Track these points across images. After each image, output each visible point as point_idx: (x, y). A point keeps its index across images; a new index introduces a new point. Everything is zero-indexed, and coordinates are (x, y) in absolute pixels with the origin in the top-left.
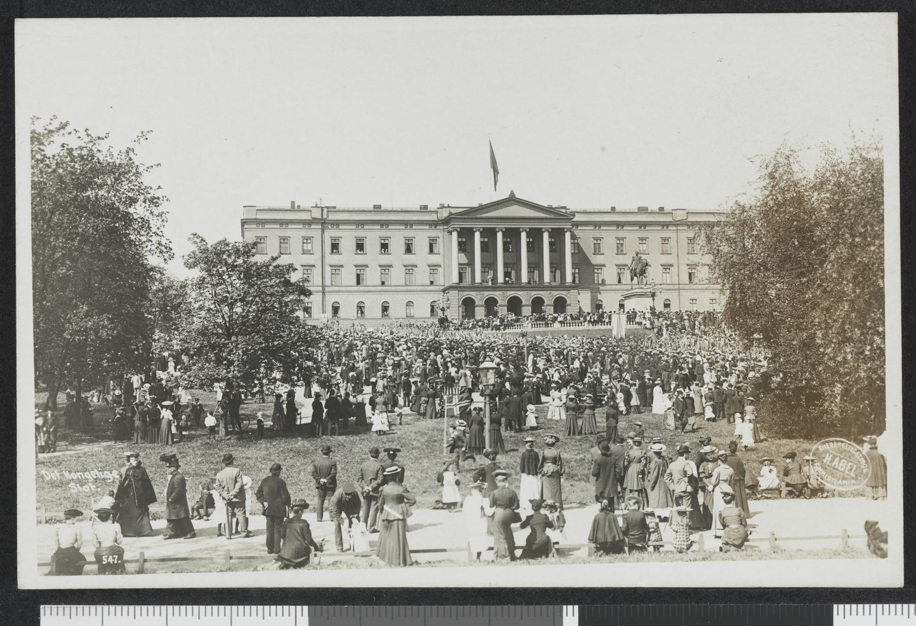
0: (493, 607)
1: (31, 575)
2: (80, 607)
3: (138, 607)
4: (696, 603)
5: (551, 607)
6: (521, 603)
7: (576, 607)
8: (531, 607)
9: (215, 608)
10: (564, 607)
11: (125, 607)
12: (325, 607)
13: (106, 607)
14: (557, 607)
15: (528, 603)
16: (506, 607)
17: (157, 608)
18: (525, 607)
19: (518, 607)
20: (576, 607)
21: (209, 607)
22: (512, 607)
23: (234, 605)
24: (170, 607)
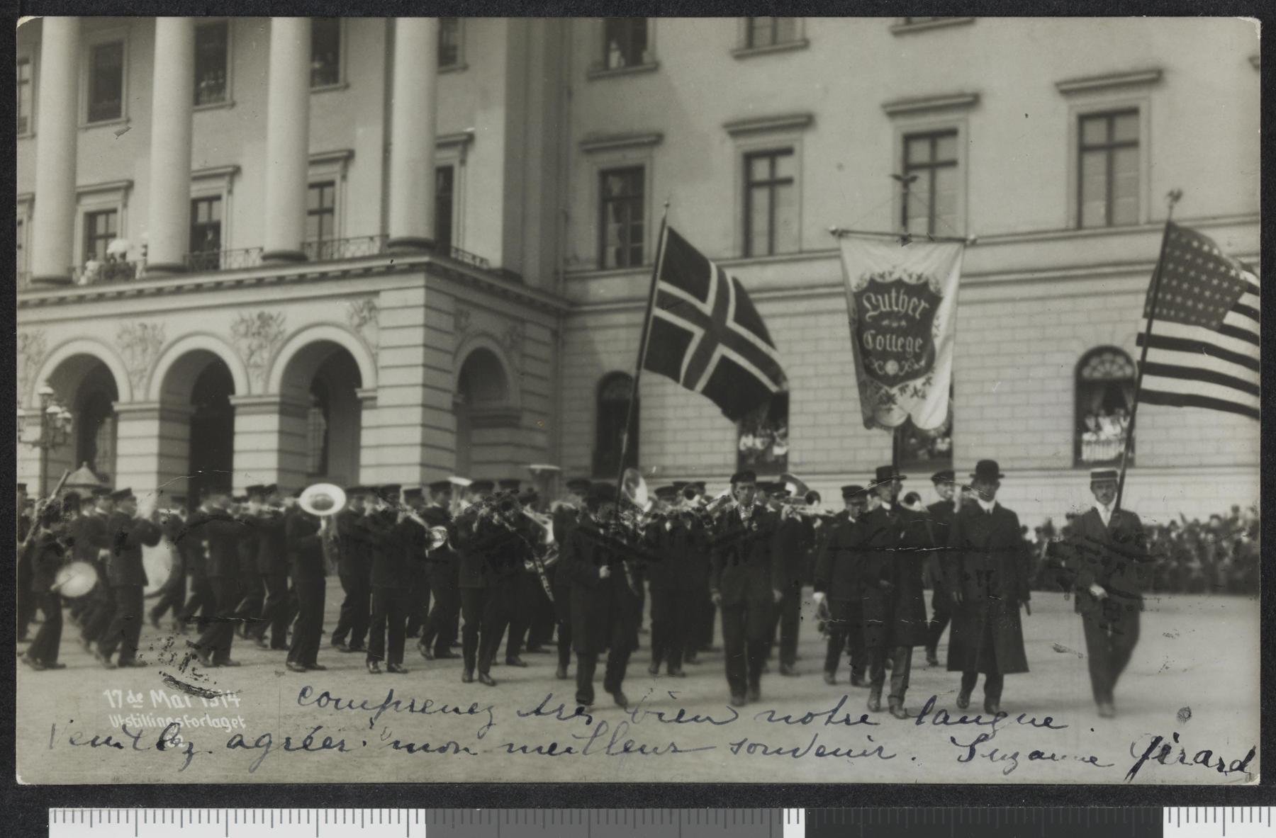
0: (684, 811)
1: (30, 769)
4: (971, 805)
6: (725, 806)
7: (802, 811)
8: (739, 811)
9: (295, 811)
10: (786, 810)
12: (449, 811)
13: (141, 811)
14: (775, 811)
16: (703, 811)
17: (213, 811)
18: (730, 811)
19: (721, 811)
20: (802, 811)
21: (286, 811)
22: (712, 811)
24: (231, 811)
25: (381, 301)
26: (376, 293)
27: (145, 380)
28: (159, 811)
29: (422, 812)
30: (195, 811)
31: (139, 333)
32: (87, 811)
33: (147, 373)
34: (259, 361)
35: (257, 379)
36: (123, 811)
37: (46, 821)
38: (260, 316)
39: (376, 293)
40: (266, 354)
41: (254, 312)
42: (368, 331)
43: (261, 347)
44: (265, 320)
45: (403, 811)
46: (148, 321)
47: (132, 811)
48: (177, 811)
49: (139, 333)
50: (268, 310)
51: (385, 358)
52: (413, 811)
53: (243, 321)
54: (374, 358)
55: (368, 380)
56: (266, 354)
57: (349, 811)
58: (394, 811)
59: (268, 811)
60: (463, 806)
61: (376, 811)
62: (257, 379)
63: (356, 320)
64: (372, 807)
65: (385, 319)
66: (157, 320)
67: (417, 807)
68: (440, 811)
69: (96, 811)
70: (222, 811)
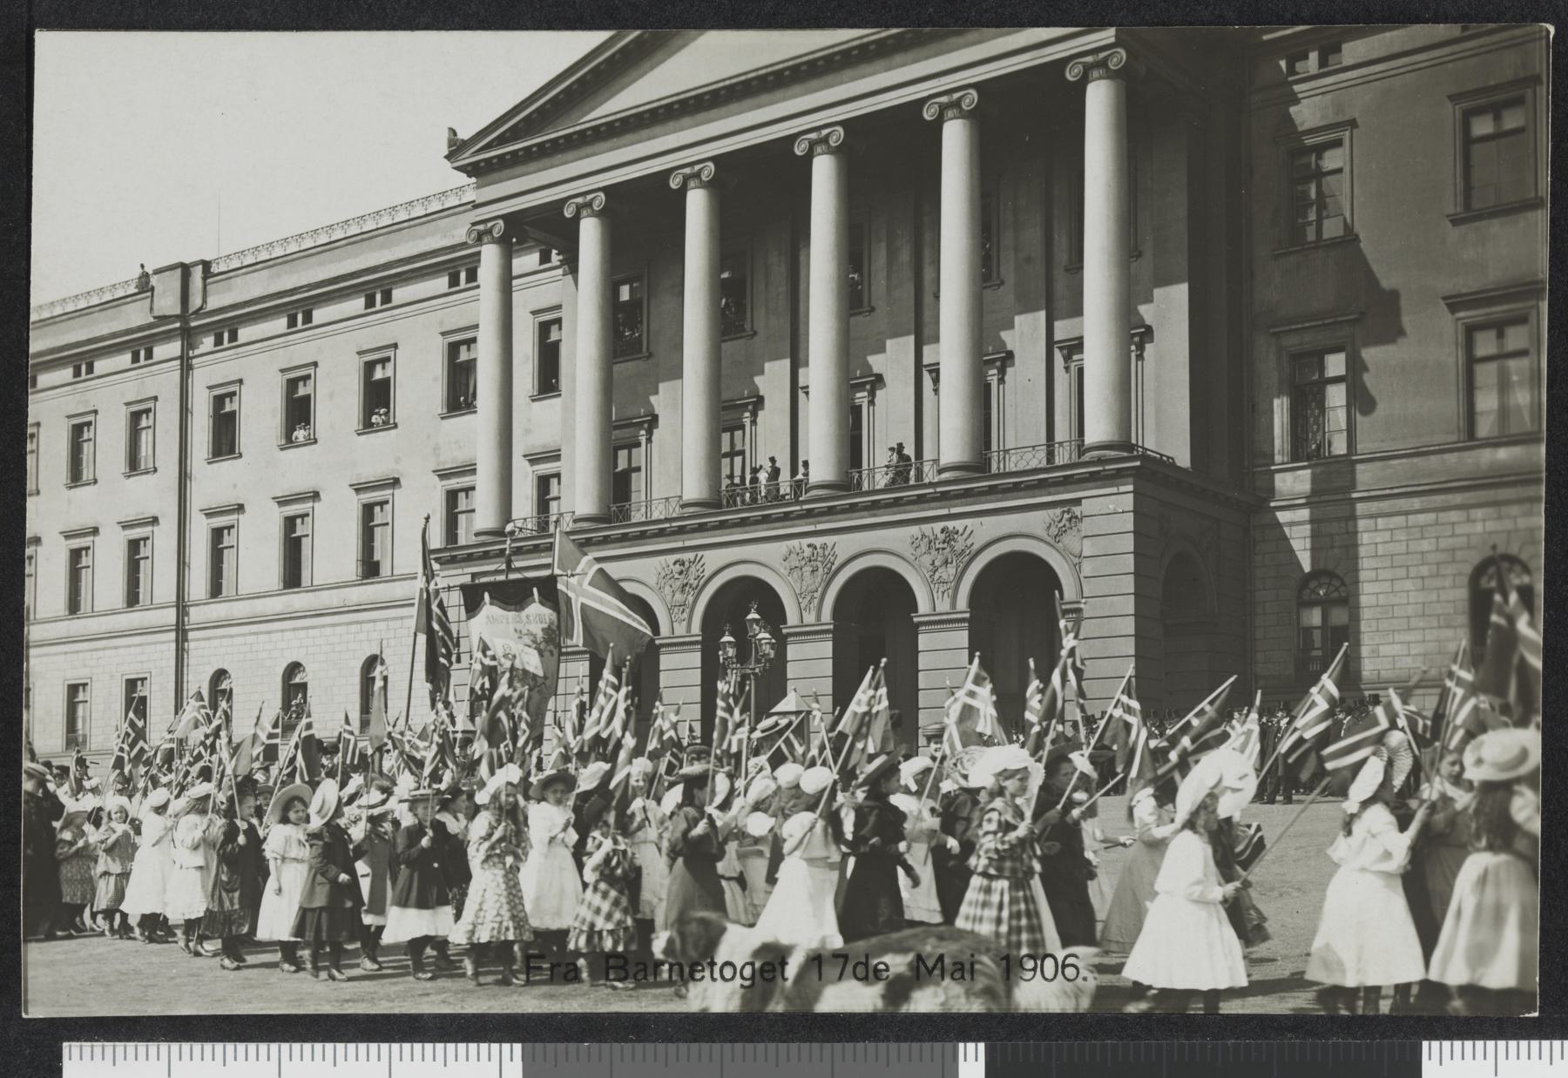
25: (1087, 507)
26: (1078, 502)
31: (808, 552)
33: (817, 595)
34: (945, 576)
35: (940, 595)
39: (1078, 502)
40: (951, 570)
41: (938, 526)
42: (1070, 540)
43: (946, 562)
44: (950, 536)
46: (818, 541)
49: (808, 552)
50: (950, 524)
51: (1087, 568)
53: (923, 536)
54: (1077, 567)
55: (1069, 592)
56: (951, 570)
63: (1054, 531)
65: (1086, 527)
66: (829, 540)
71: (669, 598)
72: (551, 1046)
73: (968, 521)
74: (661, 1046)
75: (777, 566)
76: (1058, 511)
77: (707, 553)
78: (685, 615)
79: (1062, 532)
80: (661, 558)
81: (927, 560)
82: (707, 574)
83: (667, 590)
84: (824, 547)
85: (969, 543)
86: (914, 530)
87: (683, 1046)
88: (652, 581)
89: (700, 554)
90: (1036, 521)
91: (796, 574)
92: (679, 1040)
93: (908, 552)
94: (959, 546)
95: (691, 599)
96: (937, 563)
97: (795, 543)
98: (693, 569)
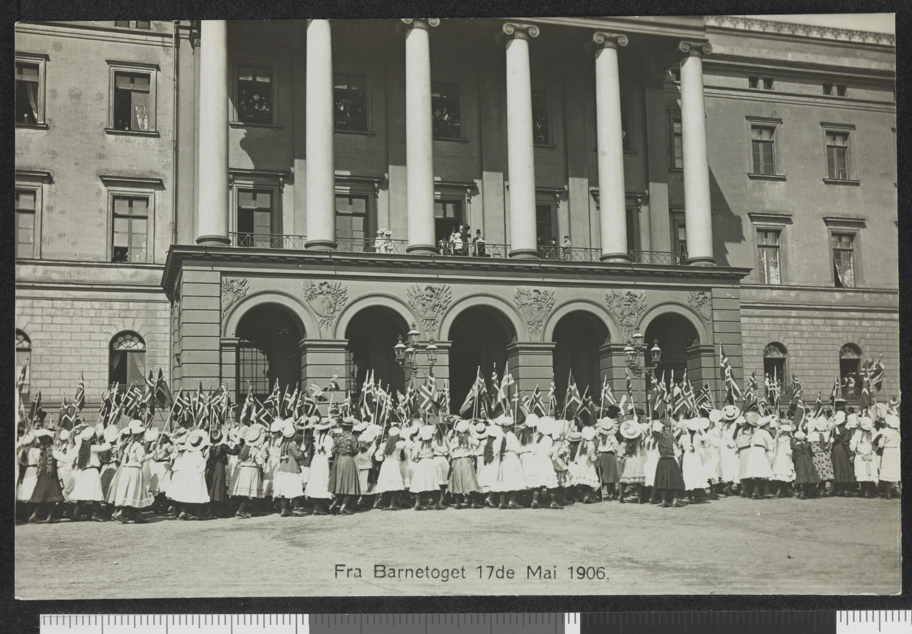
2: (80, 616)
3: (138, 616)
5: (553, 614)
9: (215, 616)
11: (125, 616)
15: (529, 611)
17: (157, 616)
21: (209, 616)
23: (234, 613)
24: (170, 616)
27: (541, 329)
28: (119, 616)
29: (306, 616)
30: (144, 616)
31: (534, 295)
32: (67, 616)
33: (544, 323)
35: (625, 332)
36: (93, 616)
37: (38, 624)
38: (629, 293)
41: (625, 291)
44: (632, 298)
45: (293, 616)
46: (542, 289)
47: (99, 616)
48: (131, 616)
50: (633, 291)
52: (300, 616)
55: (704, 339)
57: (254, 616)
58: (287, 616)
59: (196, 616)
60: (336, 612)
61: (274, 616)
62: (625, 332)
64: (271, 612)
65: (717, 304)
67: (303, 613)
68: (319, 616)
69: (73, 616)
70: (164, 616)
71: (421, 313)
72: (326, 616)
73: (643, 291)
74: (390, 615)
75: (511, 301)
76: (697, 293)
77: (453, 286)
78: (436, 327)
79: (700, 304)
80: (414, 284)
81: (618, 311)
82: (454, 301)
83: (420, 307)
84: (546, 293)
85: (644, 303)
86: (608, 291)
87: (403, 615)
88: (406, 300)
89: (447, 285)
90: (684, 297)
91: (526, 308)
92: (401, 612)
93: (605, 304)
94: (639, 305)
95: (440, 317)
96: (625, 313)
97: (525, 288)
98: (443, 295)
